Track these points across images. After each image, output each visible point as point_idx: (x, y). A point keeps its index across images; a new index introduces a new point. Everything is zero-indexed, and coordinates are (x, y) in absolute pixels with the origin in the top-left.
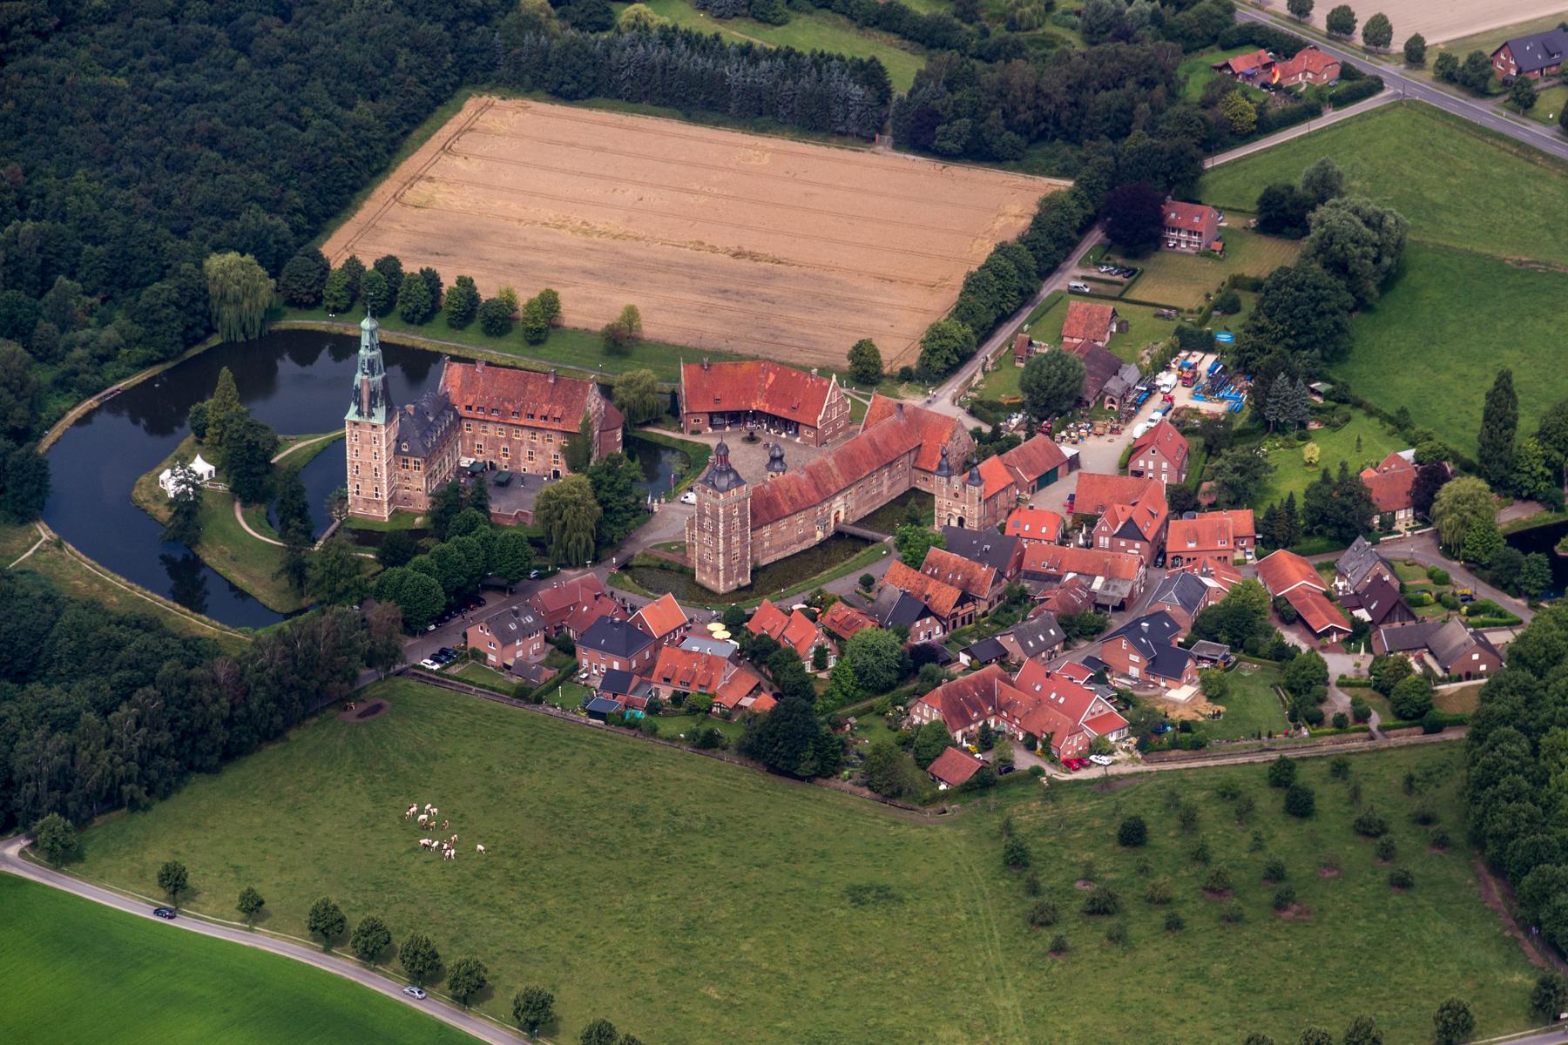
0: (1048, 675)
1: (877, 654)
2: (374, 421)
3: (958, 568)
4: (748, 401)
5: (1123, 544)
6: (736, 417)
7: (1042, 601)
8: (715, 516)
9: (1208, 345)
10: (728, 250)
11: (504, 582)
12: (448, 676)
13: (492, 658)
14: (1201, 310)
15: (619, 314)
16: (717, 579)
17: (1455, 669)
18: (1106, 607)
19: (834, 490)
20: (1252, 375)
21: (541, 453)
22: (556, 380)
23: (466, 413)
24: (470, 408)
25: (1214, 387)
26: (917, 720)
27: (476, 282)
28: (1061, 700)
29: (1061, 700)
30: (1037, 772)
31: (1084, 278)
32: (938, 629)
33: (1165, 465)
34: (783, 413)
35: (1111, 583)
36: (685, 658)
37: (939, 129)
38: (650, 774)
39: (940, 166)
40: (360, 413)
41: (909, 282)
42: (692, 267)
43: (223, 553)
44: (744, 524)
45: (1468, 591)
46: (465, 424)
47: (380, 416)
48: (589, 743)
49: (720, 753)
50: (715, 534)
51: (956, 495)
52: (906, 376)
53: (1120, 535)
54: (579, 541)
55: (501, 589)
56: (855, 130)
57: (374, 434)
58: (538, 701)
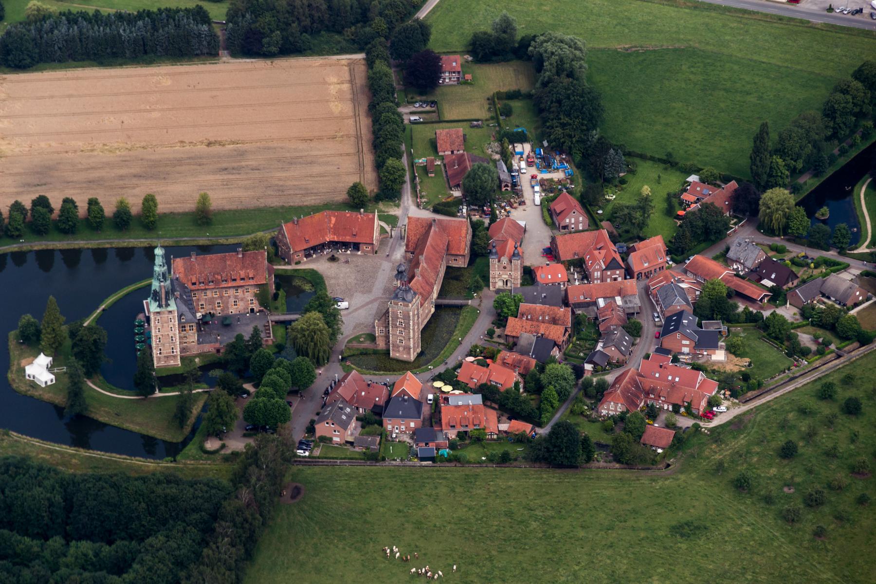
0: (661, 366)
1: (565, 379)
2: (170, 309)
3: (544, 313)
4: (323, 237)
5: (609, 273)
10: (202, 142)
12: (315, 458)
13: (336, 439)
16: (409, 353)
17: (850, 303)
21: (242, 300)
23: (193, 287)
24: (194, 284)
26: (604, 412)
28: (677, 379)
29: (677, 379)
30: (697, 427)
33: (581, 219)
34: (348, 239)
35: (628, 299)
36: (457, 410)
37: (265, 40)
38: (492, 489)
39: (269, 62)
40: (160, 306)
41: (320, 138)
43: (108, 413)
45: (803, 254)
47: (173, 307)
48: (439, 478)
49: (515, 464)
50: (407, 328)
51: (505, 268)
52: (378, 198)
53: (608, 268)
56: (205, 51)
57: (170, 316)
58: (384, 459)
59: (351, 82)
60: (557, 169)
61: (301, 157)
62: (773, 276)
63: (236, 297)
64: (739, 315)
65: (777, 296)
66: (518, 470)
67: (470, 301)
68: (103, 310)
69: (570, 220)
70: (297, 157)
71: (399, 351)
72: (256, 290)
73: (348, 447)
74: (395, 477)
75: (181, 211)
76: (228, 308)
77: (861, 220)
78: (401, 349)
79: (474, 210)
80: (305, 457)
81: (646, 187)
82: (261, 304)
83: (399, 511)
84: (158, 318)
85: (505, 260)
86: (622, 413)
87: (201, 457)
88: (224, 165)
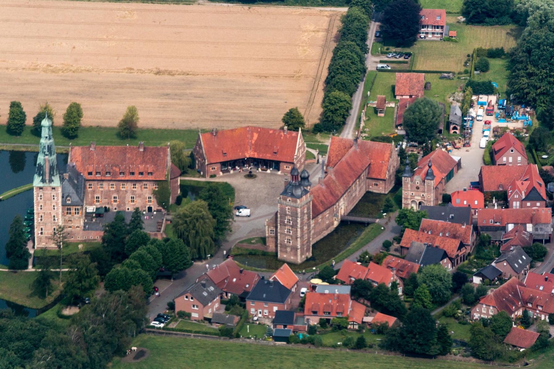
1: (441, 280)
2: (53, 185)
4: (243, 152)
5: (529, 204)
6: (233, 164)
7: (506, 241)
8: (294, 215)
9: (488, 89)
11: (169, 273)
13: (195, 315)
14: (466, 72)
16: (296, 255)
18: (541, 241)
19: (340, 195)
20: (527, 105)
22: (145, 149)
23: (89, 177)
24: (90, 173)
25: (508, 115)
27: (23, 104)
31: (381, 62)
32: (450, 265)
34: (268, 156)
39: (246, 7)
40: (43, 181)
41: (276, 76)
42: (133, 83)
44: (309, 219)
46: (88, 184)
47: (56, 182)
48: (287, 355)
49: (370, 350)
50: (294, 226)
51: (418, 188)
53: (527, 199)
54: (206, 242)
55: (169, 277)
57: (53, 193)
58: (238, 336)
60: (517, 120)
61: (250, 90)
63: (133, 193)
66: (370, 355)
69: (508, 159)
70: (246, 90)
71: (286, 252)
72: (154, 187)
73: (207, 323)
74: (244, 351)
78: (289, 249)
80: (160, 328)
85: (418, 179)
88: (168, 91)
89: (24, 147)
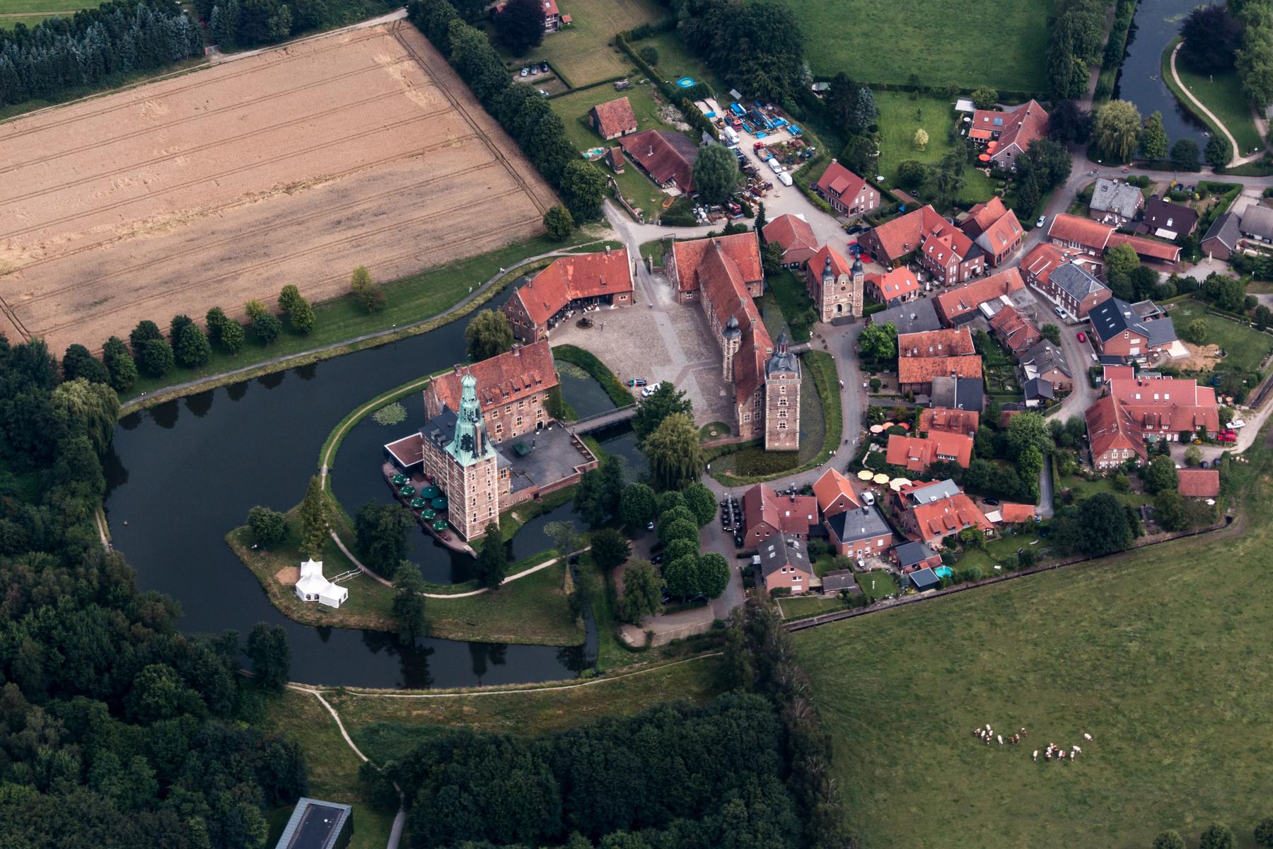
2: (488, 456)
4: (563, 295)
13: (796, 588)
15: (349, 280)
29: (1167, 397)
34: (596, 291)
36: (935, 509)
39: (280, 50)
51: (843, 289)
57: (489, 466)
59: (412, 56)
60: (773, 129)
62: (1170, 223)
63: (520, 412)
64: (1163, 287)
65: (1190, 249)
67: (809, 345)
68: (329, 471)
70: (421, 185)
72: (545, 397)
73: (815, 595)
74: (905, 623)
75: (326, 298)
76: (510, 430)
77: (1205, 120)
79: (715, 210)
81: (921, 131)
82: (551, 415)
83: (949, 671)
84: (473, 472)
85: (843, 278)
86: (1128, 460)
87: (632, 658)
88: (334, 217)
89: (260, 369)
